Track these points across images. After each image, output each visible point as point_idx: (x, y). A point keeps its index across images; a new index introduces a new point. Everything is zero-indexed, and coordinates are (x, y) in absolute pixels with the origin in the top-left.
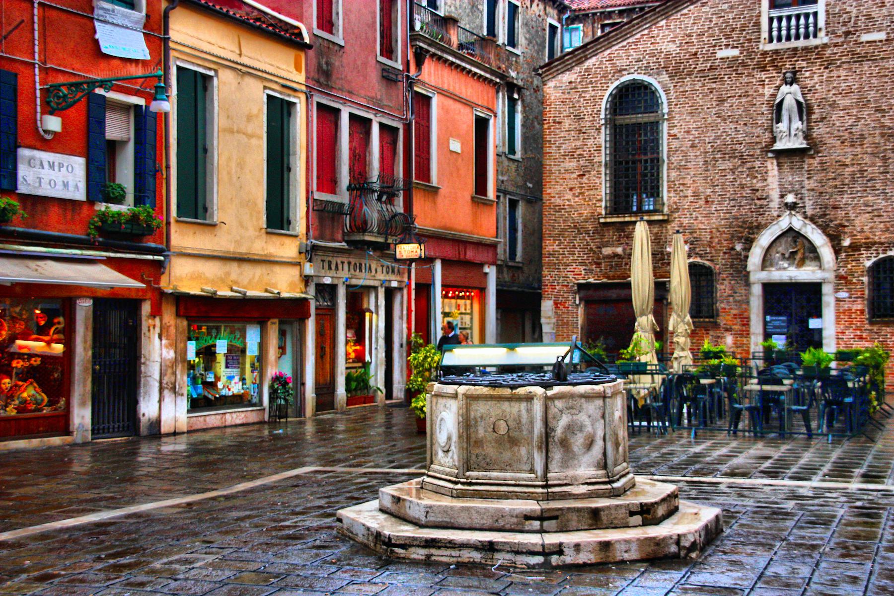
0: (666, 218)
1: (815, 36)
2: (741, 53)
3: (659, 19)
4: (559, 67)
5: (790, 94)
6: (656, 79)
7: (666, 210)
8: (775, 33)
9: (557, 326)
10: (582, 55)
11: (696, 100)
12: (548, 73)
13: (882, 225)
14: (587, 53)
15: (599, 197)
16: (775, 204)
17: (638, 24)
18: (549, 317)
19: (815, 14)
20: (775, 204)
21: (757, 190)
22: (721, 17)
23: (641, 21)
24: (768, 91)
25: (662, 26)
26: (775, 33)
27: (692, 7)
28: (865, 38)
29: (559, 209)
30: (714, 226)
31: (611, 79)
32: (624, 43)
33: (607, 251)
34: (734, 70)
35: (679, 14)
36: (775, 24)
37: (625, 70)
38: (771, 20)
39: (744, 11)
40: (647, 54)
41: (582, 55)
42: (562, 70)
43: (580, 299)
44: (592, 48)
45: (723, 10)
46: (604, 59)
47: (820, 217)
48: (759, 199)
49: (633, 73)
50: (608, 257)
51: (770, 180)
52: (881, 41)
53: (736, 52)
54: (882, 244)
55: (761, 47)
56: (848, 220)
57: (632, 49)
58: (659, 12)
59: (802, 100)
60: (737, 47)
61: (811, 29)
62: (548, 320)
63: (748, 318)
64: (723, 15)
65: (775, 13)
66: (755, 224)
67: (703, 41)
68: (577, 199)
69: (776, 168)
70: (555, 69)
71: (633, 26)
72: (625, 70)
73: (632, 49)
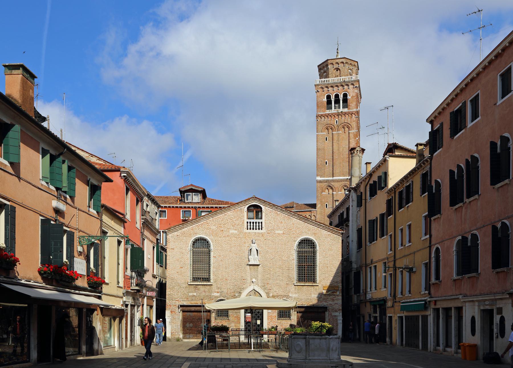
0: (212, 284)
1: (262, 229)
2: (238, 232)
3: (210, 218)
4: (173, 230)
5: (254, 247)
6: (209, 237)
7: (212, 281)
8: (249, 227)
9: (171, 320)
10: (182, 227)
11: (222, 246)
12: (169, 232)
13: (282, 290)
14: (184, 226)
15: (188, 276)
16: (249, 281)
17: (202, 218)
18: (169, 316)
19: (261, 223)
20: (249, 281)
21: (243, 277)
22: (231, 219)
23: (204, 218)
24: (247, 245)
25: (211, 220)
26: (249, 227)
27: (221, 215)
28: (277, 232)
29: (172, 279)
30: (229, 287)
31: (192, 236)
32: (197, 224)
33: (191, 294)
34: (235, 237)
35: (217, 217)
36: (249, 224)
37: (197, 233)
38: (247, 222)
39: (239, 218)
40: (206, 229)
41: (182, 227)
42: (174, 231)
43: (181, 310)
44: (186, 224)
45: (232, 217)
46: (190, 229)
47: (263, 286)
48: (243, 280)
49: (200, 235)
50: (191, 296)
51: (247, 274)
52: (281, 233)
53: (236, 232)
54: (282, 296)
55: (244, 231)
56: (272, 288)
57: (200, 226)
58: (210, 215)
59: (257, 249)
60: (237, 230)
61: (260, 227)
62: (168, 317)
63: (240, 318)
64: (232, 219)
65: (249, 221)
66: (242, 287)
67: (225, 227)
68: (179, 276)
69: (249, 270)
70: (172, 230)
71: (201, 219)
72: (197, 233)
73: (200, 226)
